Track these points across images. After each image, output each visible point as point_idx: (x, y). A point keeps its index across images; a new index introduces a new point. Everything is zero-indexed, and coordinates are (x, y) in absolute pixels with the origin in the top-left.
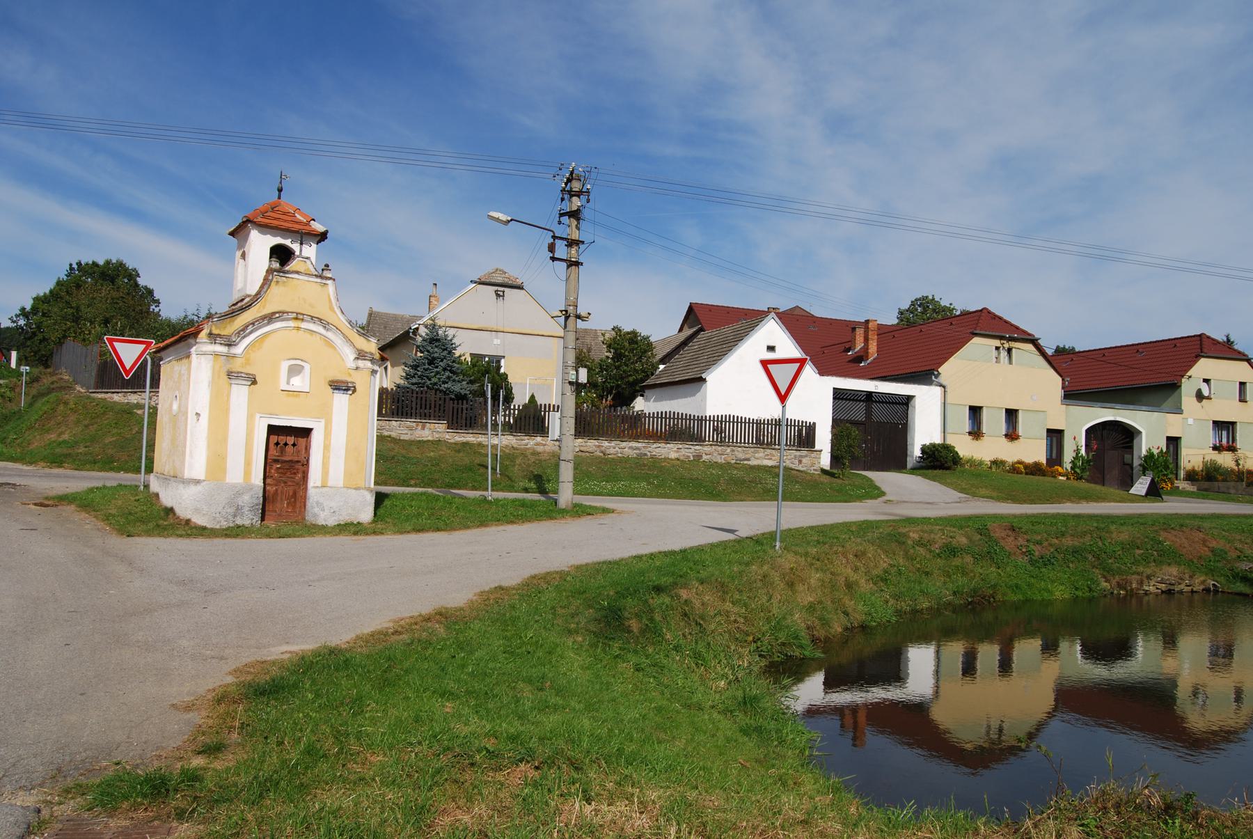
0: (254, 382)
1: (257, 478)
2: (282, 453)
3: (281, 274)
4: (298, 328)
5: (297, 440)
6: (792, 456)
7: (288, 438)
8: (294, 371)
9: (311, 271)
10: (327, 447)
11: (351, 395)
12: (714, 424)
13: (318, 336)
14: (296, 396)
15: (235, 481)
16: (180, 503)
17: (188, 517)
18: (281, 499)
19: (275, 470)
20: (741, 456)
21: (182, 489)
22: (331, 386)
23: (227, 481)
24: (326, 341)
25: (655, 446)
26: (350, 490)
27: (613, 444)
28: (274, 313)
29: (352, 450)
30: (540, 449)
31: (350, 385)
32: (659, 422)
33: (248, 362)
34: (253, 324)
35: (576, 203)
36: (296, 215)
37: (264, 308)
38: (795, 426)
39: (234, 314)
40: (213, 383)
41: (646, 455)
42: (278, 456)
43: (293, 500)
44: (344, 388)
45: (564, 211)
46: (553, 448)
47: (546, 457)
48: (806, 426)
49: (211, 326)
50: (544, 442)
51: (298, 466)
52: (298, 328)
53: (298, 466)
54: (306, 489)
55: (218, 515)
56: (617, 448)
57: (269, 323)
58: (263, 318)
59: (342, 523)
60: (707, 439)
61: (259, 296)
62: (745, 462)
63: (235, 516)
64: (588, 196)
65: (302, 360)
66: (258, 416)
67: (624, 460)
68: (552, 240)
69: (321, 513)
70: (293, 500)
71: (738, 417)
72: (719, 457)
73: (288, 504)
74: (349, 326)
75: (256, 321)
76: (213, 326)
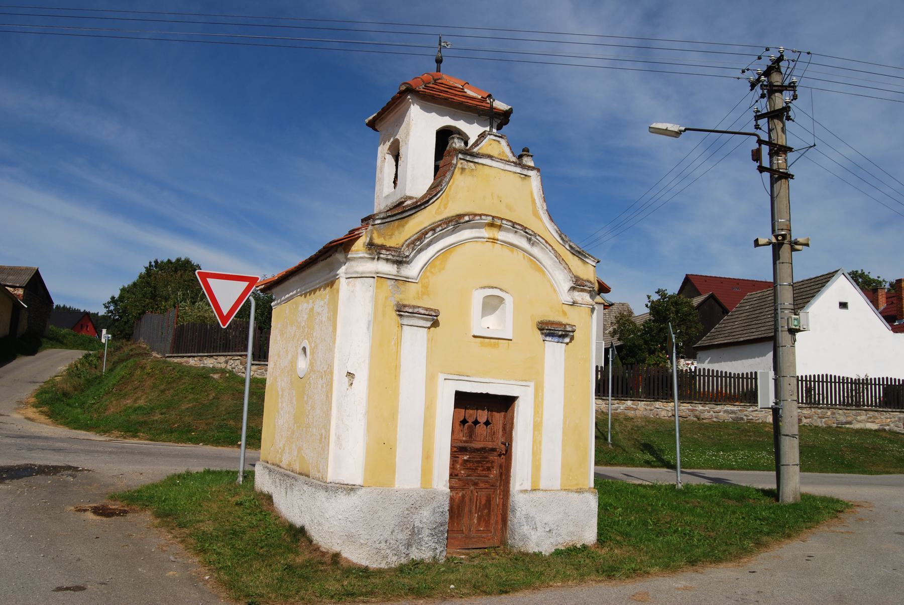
0: (435, 324)
1: (441, 481)
2: (471, 437)
3: (468, 158)
4: (494, 240)
5: (492, 416)
6: (896, 419)
7: (480, 412)
8: (491, 305)
9: (507, 156)
10: (537, 427)
11: (567, 344)
12: (806, 384)
13: (521, 253)
14: (495, 345)
15: (407, 486)
16: (320, 524)
17: (336, 549)
18: (470, 511)
19: (461, 465)
20: (843, 419)
21: (324, 499)
22: (541, 329)
23: (398, 485)
24: (531, 260)
25: (751, 409)
26: (571, 495)
27: (707, 408)
28: (460, 216)
29: (570, 430)
30: (631, 414)
31: (569, 329)
32: (845, 387)
33: (425, 291)
34: (433, 230)
35: (780, 100)
36: (466, 90)
37: (445, 208)
38: (879, 385)
39: (404, 215)
40: (376, 321)
41: (742, 419)
42: (466, 442)
43: (486, 511)
44: (560, 333)
45: (760, 113)
46: (645, 413)
47: (640, 423)
48: (883, 384)
49: (372, 233)
50: (635, 407)
51: (493, 457)
52: (494, 240)
53: (493, 457)
54: (506, 493)
55: (383, 545)
56: (712, 412)
57: (453, 231)
58: (447, 221)
59: (561, 548)
60: (821, 403)
61: (439, 188)
62: (848, 426)
63: (409, 545)
64: (795, 91)
65: (501, 289)
66: (441, 377)
67: (720, 426)
68: (757, 146)
69: (533, 533)
70: (486, 511)
71: (839, 377)
72: (819, 420)
73: (479, 518)
74: (559, 239)
75: (438, 226)
76: (375, 232)
